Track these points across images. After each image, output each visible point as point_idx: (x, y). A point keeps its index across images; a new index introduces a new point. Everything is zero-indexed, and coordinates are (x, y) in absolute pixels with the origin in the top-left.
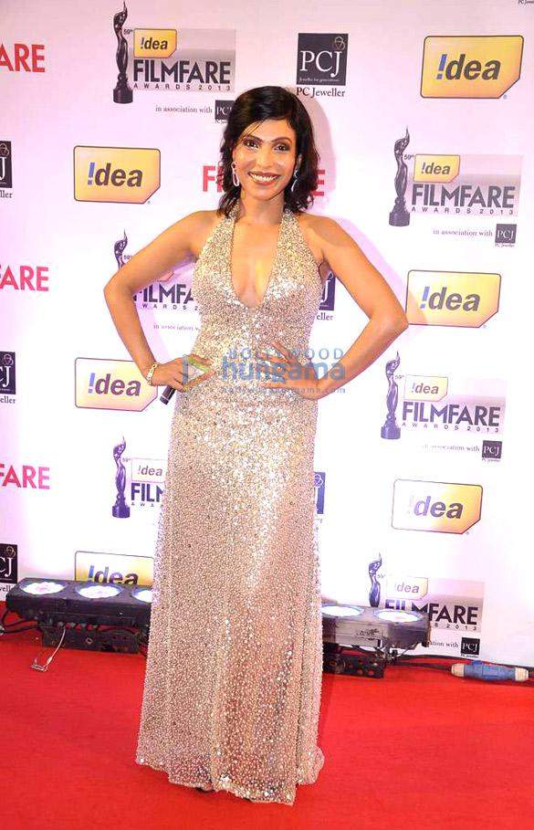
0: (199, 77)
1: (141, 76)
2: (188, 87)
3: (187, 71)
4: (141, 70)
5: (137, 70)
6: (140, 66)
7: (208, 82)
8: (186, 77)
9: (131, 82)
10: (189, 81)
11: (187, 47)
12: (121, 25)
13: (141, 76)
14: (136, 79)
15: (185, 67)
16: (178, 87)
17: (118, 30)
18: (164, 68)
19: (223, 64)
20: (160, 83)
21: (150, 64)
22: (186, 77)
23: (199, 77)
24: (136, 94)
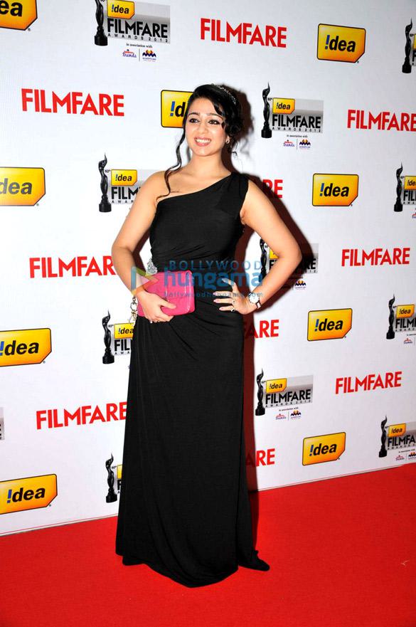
0: (306, 124)
1: (276, 123)
2: (300, 130)
3: (300, 121)
4: (276, 120)
5: (274, 120)
6: (276, 118)
7: (310, 127)
8: (299, 124)
9: (271, 126)
10: (301, 126)
11: (301, 108)
12: (266, 97)
13: (276, 123)
14: (273, 125)
15: (299, 119)
16: (295, 130)
17: (265, 98)
18: (288, 119)
20: (286, 127)
21: (281, 117)
22: (299, 124)
23: (306, 124)
24: (273, 133)
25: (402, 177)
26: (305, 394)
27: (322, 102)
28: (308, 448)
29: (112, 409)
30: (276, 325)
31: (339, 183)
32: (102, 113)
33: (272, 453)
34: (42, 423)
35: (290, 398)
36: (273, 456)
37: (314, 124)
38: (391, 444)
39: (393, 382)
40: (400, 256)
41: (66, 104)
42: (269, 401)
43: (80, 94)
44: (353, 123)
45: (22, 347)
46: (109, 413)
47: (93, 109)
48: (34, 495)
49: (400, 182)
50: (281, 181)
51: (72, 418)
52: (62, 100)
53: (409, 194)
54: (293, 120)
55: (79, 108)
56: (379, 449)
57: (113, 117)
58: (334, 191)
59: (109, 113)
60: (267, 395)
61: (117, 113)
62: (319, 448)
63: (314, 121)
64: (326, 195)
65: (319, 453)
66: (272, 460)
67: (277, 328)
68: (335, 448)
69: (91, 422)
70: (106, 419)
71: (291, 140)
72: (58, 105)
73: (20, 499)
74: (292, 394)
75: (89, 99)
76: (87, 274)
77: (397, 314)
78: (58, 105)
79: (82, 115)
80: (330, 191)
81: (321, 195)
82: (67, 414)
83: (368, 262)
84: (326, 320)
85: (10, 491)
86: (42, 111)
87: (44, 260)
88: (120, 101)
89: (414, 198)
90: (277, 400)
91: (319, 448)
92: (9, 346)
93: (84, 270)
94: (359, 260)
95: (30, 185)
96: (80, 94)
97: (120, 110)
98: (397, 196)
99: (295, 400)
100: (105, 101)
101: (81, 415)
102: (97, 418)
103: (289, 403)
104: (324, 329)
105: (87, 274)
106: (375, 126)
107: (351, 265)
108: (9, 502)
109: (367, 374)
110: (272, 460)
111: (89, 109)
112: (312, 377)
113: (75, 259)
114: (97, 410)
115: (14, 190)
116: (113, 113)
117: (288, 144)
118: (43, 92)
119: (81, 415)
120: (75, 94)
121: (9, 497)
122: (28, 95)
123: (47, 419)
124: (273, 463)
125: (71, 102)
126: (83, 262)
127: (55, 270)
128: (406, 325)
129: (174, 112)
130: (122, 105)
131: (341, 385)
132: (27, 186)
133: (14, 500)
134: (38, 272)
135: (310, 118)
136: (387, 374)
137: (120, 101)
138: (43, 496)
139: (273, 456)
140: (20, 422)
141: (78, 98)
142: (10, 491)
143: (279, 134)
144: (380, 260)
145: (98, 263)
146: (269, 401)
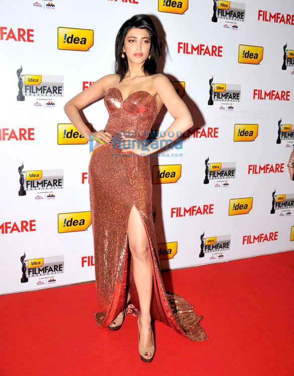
0: (236, 16)
1: (220, 14)
5: (219, 12)
8: (232, 16)
13: (220, 14)
16: (230, 19)
18: (226, 13)
19: (242, 13)
22: (232, 16)
23: (236, 16)
25: (287, 50)
26: (231, 173)
27: (244, 5)
28: (232, 206)
30: (216, 130)
31: (253, 51)
33: (212, 207)
34: (85, 180)
35: (223, 175)
36: (213, 209)
37: (240, 16)
38: (277, 206)
39: (279, 169)
40: (285, 96)
42: (212, 176)
44: (261, 17)
45: (76, 134)
48: (78, 223)
49: (285, 53)
50: (222, 47)
53: (290, 60)
54: (229, 13)
56: (271, 209)
58: (250, 55)
60: (211, 172)
62: (238, 206)
63: (240, 15)
64: (246, 57)
65: (238, 209)
66: (212, 211)
67: (217, 132)
68: (247, 207)
71: (228, 24)
73: (71, 225)
74: (224, 173)
77: (283, 130)
80: (248, 55)
81: (243, 57)
83: (267, 98)
84: (244, 130)
85: (65, 220)
89: (293, 62)
90: (216, 175)
91: (238, 206)
92: (69, 132)
94: (263, 96)
95: (85, 39)
98: (283, 61)
99: (226, 176)
103: (222, 177)
104: (243, 135)
106: (272, 20)
107: (258, 99)
108: (64, 226)
109: (266, 164)
110: (212, 211)
112: (235, 163)
115: (76, 42)
117: (226, 26)
121: (65, 223)
124: (212, 213)
128: (287, 136)
129: (165, 4)
131: (251, 169)
132: (84, 40)
133: (68, 225)
135: (238, 13)
136: (277, 165)
138: (83, 224)
139: (213, 209)
142: (65, 220)
143: (221, 21)
144: (274, 97)
146: (212, 176)
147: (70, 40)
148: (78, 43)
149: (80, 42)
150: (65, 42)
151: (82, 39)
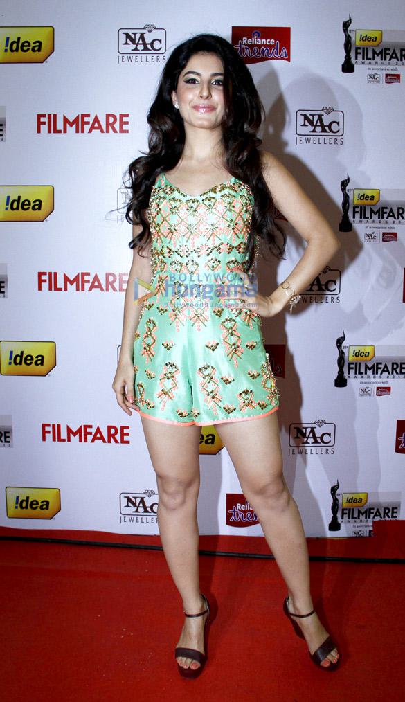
29: (113, 431)
32: (108, 131)
41: (74, 126)
43: (88, 115)
46: (109, 435)
47: (100, 127)
51: (75, 434)
52: (71, 120)
55: (87, 127)
57: (119, 134)
59: (115, 131)
61: (122, 131)
69: (93, 441)
70: (107, 441)
72: (68, 125)
75: (96, 119)
76: (90, 290)
78: (68, 125)
79: (89, 134)
82: (69, 431)
85: (18, 498)
86: (54, 132)
87: (50, 274)
88: (125, 119)
93: (87, 286)
96: (88, 115)
97: (125, 127)
100: (111, 120)
101: (82, 433)
102: (98, 438)
105: (90, 290)
111: (96, 128)
113: (78, 275)
114: (98, 430)
116: (118, 131)
118: (55, 116)
119: (82, 433)
120: (83, 116)
122: (42, 119)
123: (51, 432)
125: (79, 123)
126: (86, 278)
127: (61, 284)
130: (127, 123)
134: (45, 286)
137: (125, 119)
140: (26, 434)
141: (86, 119)
145: (101, 280)
147: (15, 205)
148: (28, 208)
149: (31, 206)
150: (7, 209)
151: (35, 202)
